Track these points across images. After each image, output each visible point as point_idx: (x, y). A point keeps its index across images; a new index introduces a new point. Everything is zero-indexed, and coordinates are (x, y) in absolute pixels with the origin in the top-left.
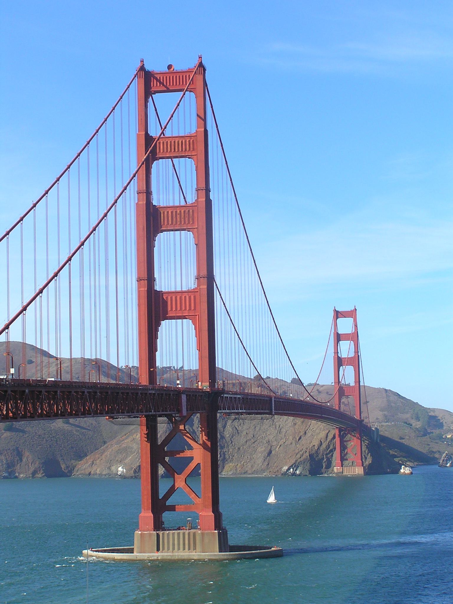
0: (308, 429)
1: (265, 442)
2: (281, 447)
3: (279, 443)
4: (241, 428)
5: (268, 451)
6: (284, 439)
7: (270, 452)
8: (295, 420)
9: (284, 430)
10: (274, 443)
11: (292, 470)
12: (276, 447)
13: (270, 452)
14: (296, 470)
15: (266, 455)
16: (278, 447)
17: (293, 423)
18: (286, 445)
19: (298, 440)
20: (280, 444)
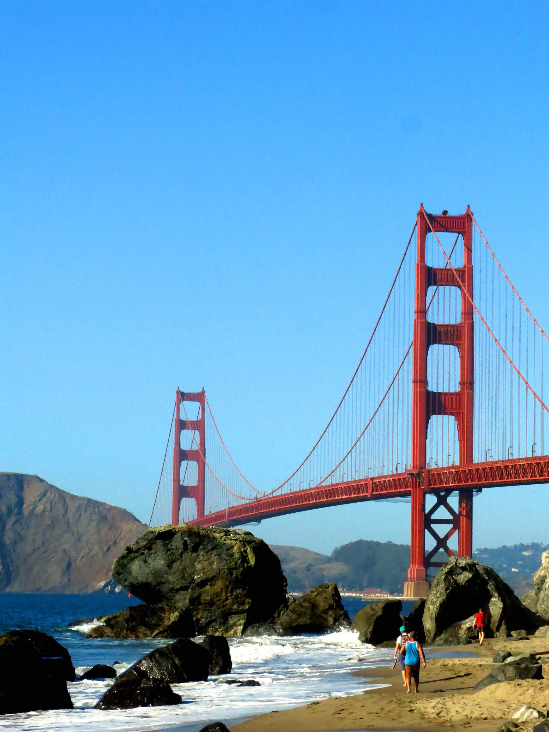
2: (83, 559)
5: (66, 563)
6: (87, 549)
9: (84, 538)
10: (73, 554)
12: (76, 560)
15: (65, 568)
16: (80, 558)
17: (97, 530)
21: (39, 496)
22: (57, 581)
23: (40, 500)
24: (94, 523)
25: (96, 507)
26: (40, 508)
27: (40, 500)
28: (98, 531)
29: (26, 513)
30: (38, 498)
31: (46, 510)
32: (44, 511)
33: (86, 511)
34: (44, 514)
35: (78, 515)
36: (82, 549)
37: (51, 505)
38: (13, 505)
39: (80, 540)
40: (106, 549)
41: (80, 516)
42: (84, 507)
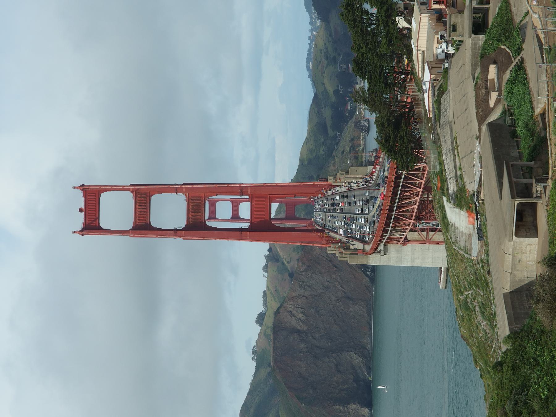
0: (326, 259)
1: (338, 304)
2: (344, 287)
3: (339, 289)
4: (322, 331)
6: (336, 283)
7: (349, 298)
8: (317, 272)
10: (340, 294)
11: (368, 273)
12: (345, 292)
13: (349, 298)
14: (369, 268)
15: (351, 302)
16: (343, 290)
18: (342, 282)
19: (337, 269)
20: (341, 288)
21: (291, 317)
22: (362, 309)
23: (295, 316)
24: (314, 275)
25: (300, 274)
26: (300, 315)
27: (295, 316)
28: (320, 273)
29: (305, 328)
30: (293, 317)
31: (303, 312)
32: (304, 314)
33: (304, 282)
34: (306, 314)
35: (307, 287)
36: (336, 287)
37: (299, 308)
38: (298, 338)
39: (328, 288)
40: (336, 269)
41: (309, 286)
42: (301, 283)
